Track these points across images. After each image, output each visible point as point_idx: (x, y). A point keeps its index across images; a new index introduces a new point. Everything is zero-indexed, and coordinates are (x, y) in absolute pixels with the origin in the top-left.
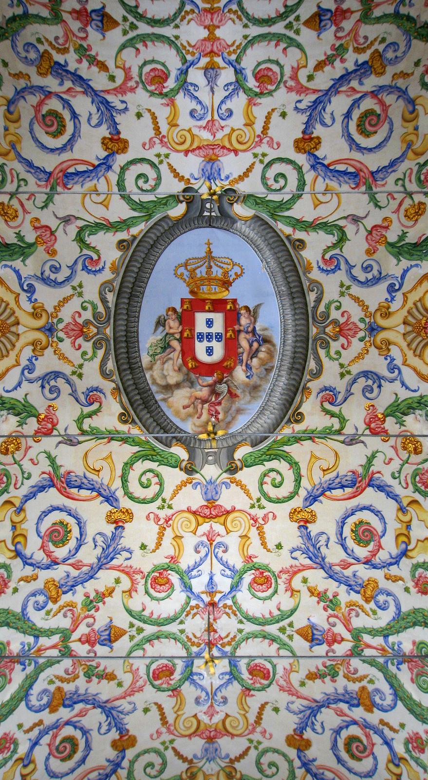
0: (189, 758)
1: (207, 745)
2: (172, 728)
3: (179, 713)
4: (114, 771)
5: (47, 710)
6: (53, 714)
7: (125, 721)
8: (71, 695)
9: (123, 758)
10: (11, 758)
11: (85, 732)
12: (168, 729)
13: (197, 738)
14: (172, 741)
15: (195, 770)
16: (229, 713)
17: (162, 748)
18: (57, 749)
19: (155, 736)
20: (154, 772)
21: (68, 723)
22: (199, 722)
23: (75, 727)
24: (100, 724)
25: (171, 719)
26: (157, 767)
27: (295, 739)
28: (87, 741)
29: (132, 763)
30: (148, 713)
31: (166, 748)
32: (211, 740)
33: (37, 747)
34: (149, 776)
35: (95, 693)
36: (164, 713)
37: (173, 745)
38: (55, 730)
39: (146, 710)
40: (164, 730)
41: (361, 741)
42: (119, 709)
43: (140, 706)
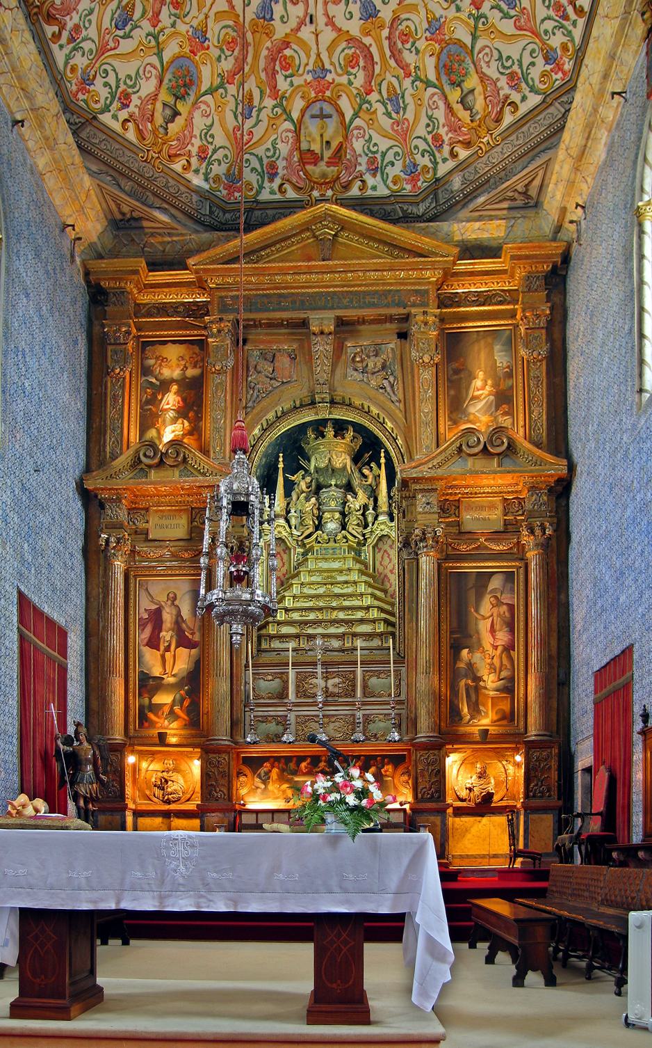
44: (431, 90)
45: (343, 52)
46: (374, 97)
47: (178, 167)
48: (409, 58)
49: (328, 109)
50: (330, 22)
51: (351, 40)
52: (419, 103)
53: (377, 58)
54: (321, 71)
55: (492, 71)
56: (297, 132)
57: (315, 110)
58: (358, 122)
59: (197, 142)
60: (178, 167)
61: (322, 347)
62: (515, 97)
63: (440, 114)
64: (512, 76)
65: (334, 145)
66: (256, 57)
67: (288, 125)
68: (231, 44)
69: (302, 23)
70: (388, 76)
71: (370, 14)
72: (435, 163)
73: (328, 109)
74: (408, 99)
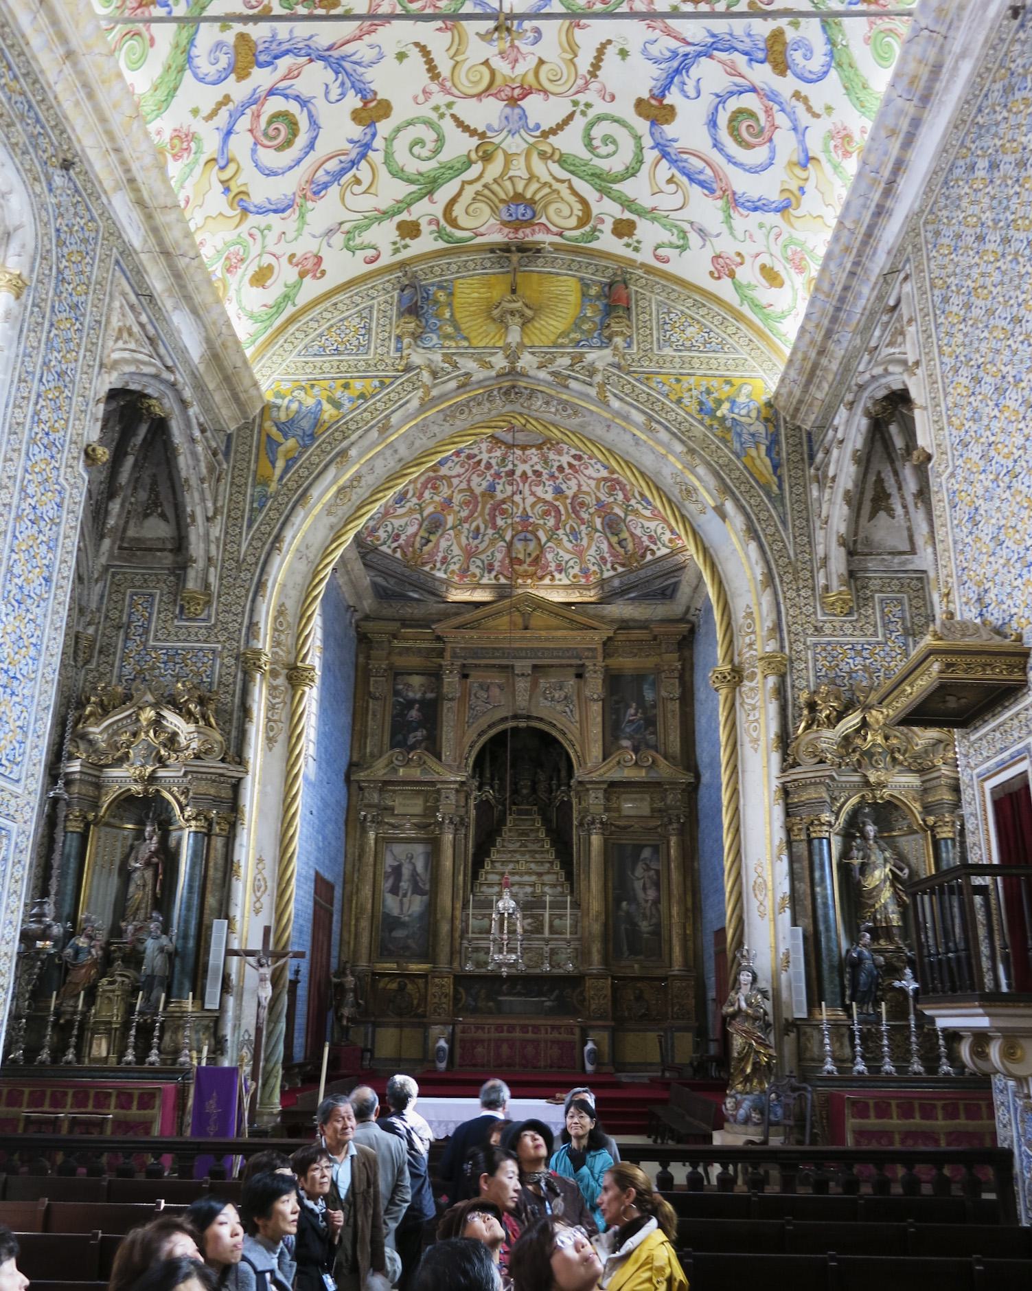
0: (480, 131)
1: (508, 110)
2: (448, 84)
3: (458, 58)
4: (363, 156)
5: (233, 77)
6: (243, 82)
7: (368, 78)
8: (266, 45)
9: (374, 135)
10: (196, 162)
11: (303, 103)
12: (442, 85)
13: (491, 98)
14: (450, 105)
15: (490, 148)
16: (544, 58)
17: (434, 116)
18: (265, 134)
19: (421, 98)
20: (425, 153)
21: (271, 92)
22: (493, 73)
23: (286, 97)
24: (327, 86)
25: (444, 68)
26: (431, 145)
27: (652, 106)
28: (310, 116)
29: (389, 141)
30: (405, 61)
31: (442, 116)
32: (513, 101)
33: (233, 137)
34: (419, 158)
35: (307, 35)
36: (432, 60)
37: (452, 111)
38: (254, 107)
39: (401, 56)
40: (434, 87)
41: (758, 120)
42: (354, 58)
43: (391, 51)
44: (598, 534)
45: (539, 508)
46: (561, 532)
47: (427, 568)
48: (585, 516)
49: (529, 536)
50: (533, 494)
51: (546, 502)
52: (591, 539)
53: (563, 511)
54: (525, 516)
55: (638, 532)
56: (510, 545)
57: (522, 536)
58: (549, 544)
59: (441, 555)
60: (427, 568)
61: (522, 685)
62: (653, 547)
63: (605, 546)
64: (651, 537)
65: (534, 555)
66: (483, 508)
67: (502, 543)
68: (467, 503)
69: (514, 494)
70: (570, 522)
71: (558, 491)
72: (602, 571)
73: (529, 536)
74: (583, 535)
